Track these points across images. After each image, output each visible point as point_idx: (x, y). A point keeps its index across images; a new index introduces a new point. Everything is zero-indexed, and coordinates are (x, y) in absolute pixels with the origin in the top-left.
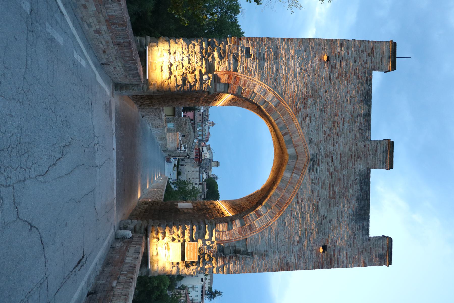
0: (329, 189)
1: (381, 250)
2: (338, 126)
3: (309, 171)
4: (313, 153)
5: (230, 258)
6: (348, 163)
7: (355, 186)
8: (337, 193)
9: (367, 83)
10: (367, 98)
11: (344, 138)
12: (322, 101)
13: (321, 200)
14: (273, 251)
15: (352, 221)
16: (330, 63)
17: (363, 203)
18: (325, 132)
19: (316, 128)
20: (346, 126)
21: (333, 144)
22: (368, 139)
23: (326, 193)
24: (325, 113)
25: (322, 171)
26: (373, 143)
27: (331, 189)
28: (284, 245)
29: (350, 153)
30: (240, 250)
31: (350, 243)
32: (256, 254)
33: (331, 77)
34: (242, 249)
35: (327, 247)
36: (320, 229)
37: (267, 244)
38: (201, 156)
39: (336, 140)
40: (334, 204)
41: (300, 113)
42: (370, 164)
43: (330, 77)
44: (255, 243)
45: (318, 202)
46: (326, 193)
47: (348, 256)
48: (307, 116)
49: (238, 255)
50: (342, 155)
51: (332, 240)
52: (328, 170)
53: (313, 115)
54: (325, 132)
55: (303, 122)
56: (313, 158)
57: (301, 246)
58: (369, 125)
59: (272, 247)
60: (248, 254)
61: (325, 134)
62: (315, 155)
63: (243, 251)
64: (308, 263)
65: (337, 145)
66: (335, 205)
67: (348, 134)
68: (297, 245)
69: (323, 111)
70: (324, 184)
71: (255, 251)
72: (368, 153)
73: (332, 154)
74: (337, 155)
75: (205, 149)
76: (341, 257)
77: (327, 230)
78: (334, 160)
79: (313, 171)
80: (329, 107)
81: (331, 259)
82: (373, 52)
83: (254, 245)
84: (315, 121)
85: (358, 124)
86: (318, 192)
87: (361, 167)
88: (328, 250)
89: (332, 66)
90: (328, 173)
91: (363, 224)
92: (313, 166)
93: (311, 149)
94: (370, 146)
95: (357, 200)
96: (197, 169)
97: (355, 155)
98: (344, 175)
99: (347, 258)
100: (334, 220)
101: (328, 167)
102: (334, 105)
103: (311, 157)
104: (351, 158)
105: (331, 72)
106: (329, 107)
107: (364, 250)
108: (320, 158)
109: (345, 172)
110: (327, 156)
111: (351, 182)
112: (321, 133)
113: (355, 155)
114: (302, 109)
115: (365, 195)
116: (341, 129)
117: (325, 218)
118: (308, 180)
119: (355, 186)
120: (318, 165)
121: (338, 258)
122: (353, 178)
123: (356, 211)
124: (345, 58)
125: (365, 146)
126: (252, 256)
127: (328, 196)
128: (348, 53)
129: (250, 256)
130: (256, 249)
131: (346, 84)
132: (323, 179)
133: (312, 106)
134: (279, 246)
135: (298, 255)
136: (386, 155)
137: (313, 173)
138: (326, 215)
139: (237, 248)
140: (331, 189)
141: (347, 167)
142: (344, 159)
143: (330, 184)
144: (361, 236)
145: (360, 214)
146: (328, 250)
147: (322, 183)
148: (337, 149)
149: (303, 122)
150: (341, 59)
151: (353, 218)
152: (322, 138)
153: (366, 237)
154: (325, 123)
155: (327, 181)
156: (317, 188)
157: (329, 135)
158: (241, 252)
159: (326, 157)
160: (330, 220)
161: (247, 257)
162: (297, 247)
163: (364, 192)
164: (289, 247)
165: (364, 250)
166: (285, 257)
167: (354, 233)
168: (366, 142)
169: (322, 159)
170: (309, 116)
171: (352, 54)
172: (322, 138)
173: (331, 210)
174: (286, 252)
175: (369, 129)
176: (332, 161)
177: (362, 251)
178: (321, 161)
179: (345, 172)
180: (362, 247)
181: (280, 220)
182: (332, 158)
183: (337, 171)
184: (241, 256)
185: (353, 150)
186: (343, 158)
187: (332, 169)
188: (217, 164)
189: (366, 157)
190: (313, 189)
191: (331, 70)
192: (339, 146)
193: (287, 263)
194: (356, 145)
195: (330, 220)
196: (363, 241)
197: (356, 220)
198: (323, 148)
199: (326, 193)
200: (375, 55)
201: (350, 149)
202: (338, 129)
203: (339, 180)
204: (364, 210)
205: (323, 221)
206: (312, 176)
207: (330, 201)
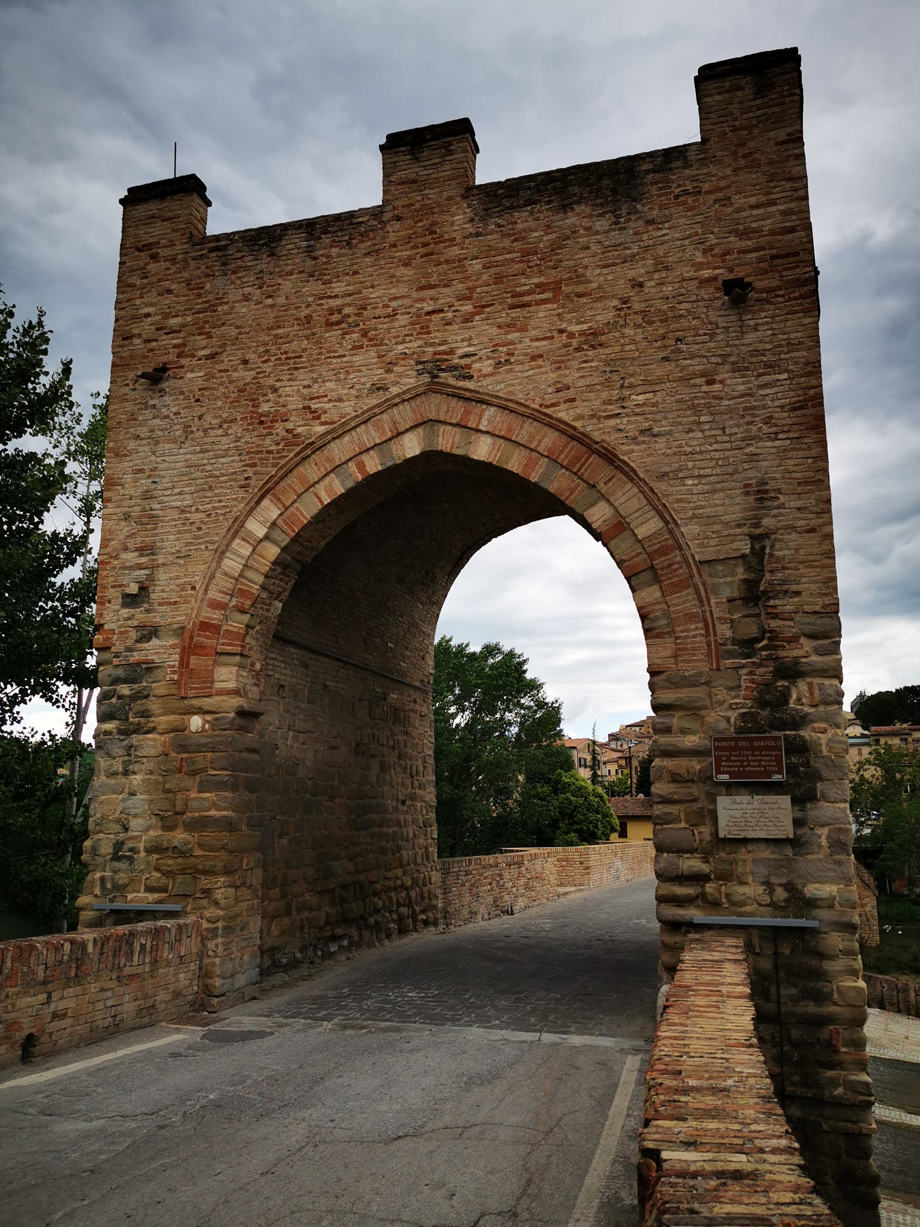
0: (528, 305)
1: (739, 94)
2: (340, 312)
3: (471, 377)
4: (415, 373)
5: (775, 616)
6: (447, 262)
7: (520, 226)
8: (542, 279)
9: (225, 248)
10: (265, 239)
11: (373, 287)
12: (269, 370)
13: (564, 326)
14: (746, 466)
15: (637, 212)
16: (170, 362)
17: (576, 190)
18: (354, 348)
19: (342, 376)
20: (339, 287)
21: (389, 316)
22: (376, 213)
23: (541, 314)
24: (301, 357)
25: (470, 339)
26: (389, 197)
27: (526, 299)
28: (724, 429)
29: (418, 261)
30: (745, 581)
31: (716, 201)
32: (757, 525)
33: (206, 352)
34: (741, 573)
35: (731, 276)
36: (665, 313)
37: (719, 486)
39: (378, 312)
40: (580, 283)
41: (299, 430)
42: (453, 193)
43: (207, 357)
44: (717, 527)
45: (571, 335)
46: (542, 312)
47: (763, 199)
48: (309, 408)
49: (762, 588)
51: (699, 267)
52: (466, 321)
53: (306, 391)
54: (354, 348)
55: (323, 419)
56: (429, 373)
57: (727, 367)
58: (338, 217)
59: (730, 469)
60: (758, 553)
61: (361, 347)
62: (420, 367)
63: (748, 569)
64: (793, 336)
65: (394, 304)
66: (579, 279)
67: (360, 277)
68: (722, 382)
69: (292, 362)
70: (510, 326)
71: (745, 530)
72: (417, 206)
73: (419, 316)
74: (422, 300)
76: (767, 225)
77: (668, 289)
78: (438, 307)
79: (469, 367)
80: (285, 347)
81: (773, 257)
82: (149, 246)
83: (726, 533)
84: (324, 382)
86: (538, 340)
87: (459, 220)
88: (741, 274)
89: (179, 356)
90: (477, 318)
91: (648, 172)
92: (455, 368)
93: (404, 381)
94: (397, 203)
95: (565, 208)
97: (425, 245)
98: (485, 267)
99: (773, 203)
100: (632, 274)
101: (459, 320)
102: (280, 331)
103: (426, 378)
104: (432, 254)
105: (193, 356)
106: (285, 347)
107: (741, 152)
108: (431, 349)
109: (477, 265)
110: (425, 330)
111: (507, 242)
112: (355, 358)
113: (425, 245)
114: (290, 426)
115: (549, 187)
116: (348, 300)
117: (625, 303)
118: (499, 378)
119: (520, 226)
120: (451, 352)
121: (772, 233)
122: (495, 236)
123: (602, 205)
124: (158, 322)
125: (399, 219)
126: (765, 536)
127: (549, 306)
128: (148, 315)
129: (768, 543)
130: (739, 526)
131: (225, 307)
132: (494, 331)
133: (280, 396)
134: (728, 445)
135: (760, 375)
136: (429, 151)
137: (476, 366)
138: (615, 303)
139: (736, 594)
140: (526, 299)
141: (460, 261)
142: (435, 274)
143: (512, 307)
144: (688, 172)
145: (614, 191)
146: (739, 273)
147: (508, 333)
148: (405, 301)
149: (323, 419)
150: (162, 332)
151: (624, 211)
152: (373, 353)
153: (692, 155)
154: (328, 352)
155: (503, 318)
156: (525, 344)
157: (365, 334)
158: (751, 576)
159: (429, 333)
160: (633, 287)
161: (771, 555)
162: (728, 382)
163: (539, 191)
164: (730, 410)
165: (741, 152)
166: (768, 420)
167: (677, 197)
168: (386, 217)
169: (432, 345)
170: (307, 403)
171: (152, 305)
172: (373, 353)
173: (600, 287)
174: (748, 418)
175: (351, 215)
176: (441, 311)
177: (745, 156)
178: (440, 345)
179: (477, 265)
180: (728, 160)
181: (632, 451)
182: (433, 312)
183: (471, 289)
184: (768, 576)
185: (408, 253)
186: (433, 280)
187: (464, 308)
189: (429, 210)
190: (528, 357)
191: (187, 356)
192: (395, 298)
193: (794, 409)
194: (395, 246)
195: (633, 287)
196: (703, 162)
197: (634, 200)
198: (400, 347)
199: (541, 314)
200: (155, 240)
201: (407, 264)
202: (346, 311)
203: (498, 279)
204: (599, 179)
205: (637, 307)
206: (486, 366)
207: (568, 297)
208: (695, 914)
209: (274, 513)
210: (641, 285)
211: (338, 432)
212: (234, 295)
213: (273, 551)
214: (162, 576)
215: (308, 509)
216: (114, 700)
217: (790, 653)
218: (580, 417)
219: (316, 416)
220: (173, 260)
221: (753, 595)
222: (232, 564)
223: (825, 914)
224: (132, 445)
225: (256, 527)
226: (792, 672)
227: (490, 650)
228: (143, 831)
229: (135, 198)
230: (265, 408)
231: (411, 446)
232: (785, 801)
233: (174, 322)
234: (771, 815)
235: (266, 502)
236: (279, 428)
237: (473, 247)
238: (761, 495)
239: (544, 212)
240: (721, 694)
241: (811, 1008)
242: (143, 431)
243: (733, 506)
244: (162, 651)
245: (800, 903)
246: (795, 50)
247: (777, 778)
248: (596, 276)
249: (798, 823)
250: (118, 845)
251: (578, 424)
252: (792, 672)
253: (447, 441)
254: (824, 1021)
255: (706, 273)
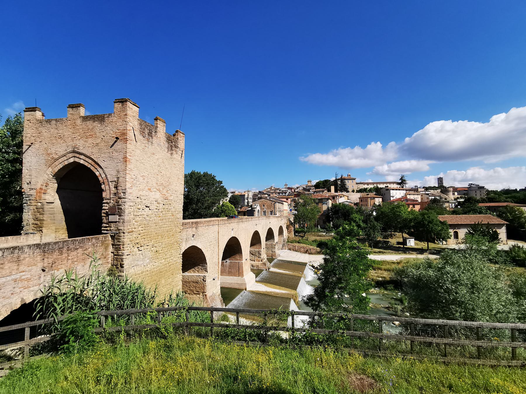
60: (118, 180)
70: (85, 141)
75: (296, 191)
109: (81, 130)
179: (81, 130)
206: (82, 148)
211: (60, 158)
212: (43, 131)
214: (33, 180)
215: (56, 170)
220: (33, 123)
223: (121, 231)
224: (27, 157)
227: (206, 175)
228: (31, 221)
231: (72, 160)
236: (51, 156)
237: (81, 127)
238: (118, 172)
239: (91, 122)
240: (112, 201)
241: (118, 243)
242: (29, 154)
243: (114, 173)
248: (98, 134)
252: (120, 198)
253: (77, 160)
254: (120, 245)
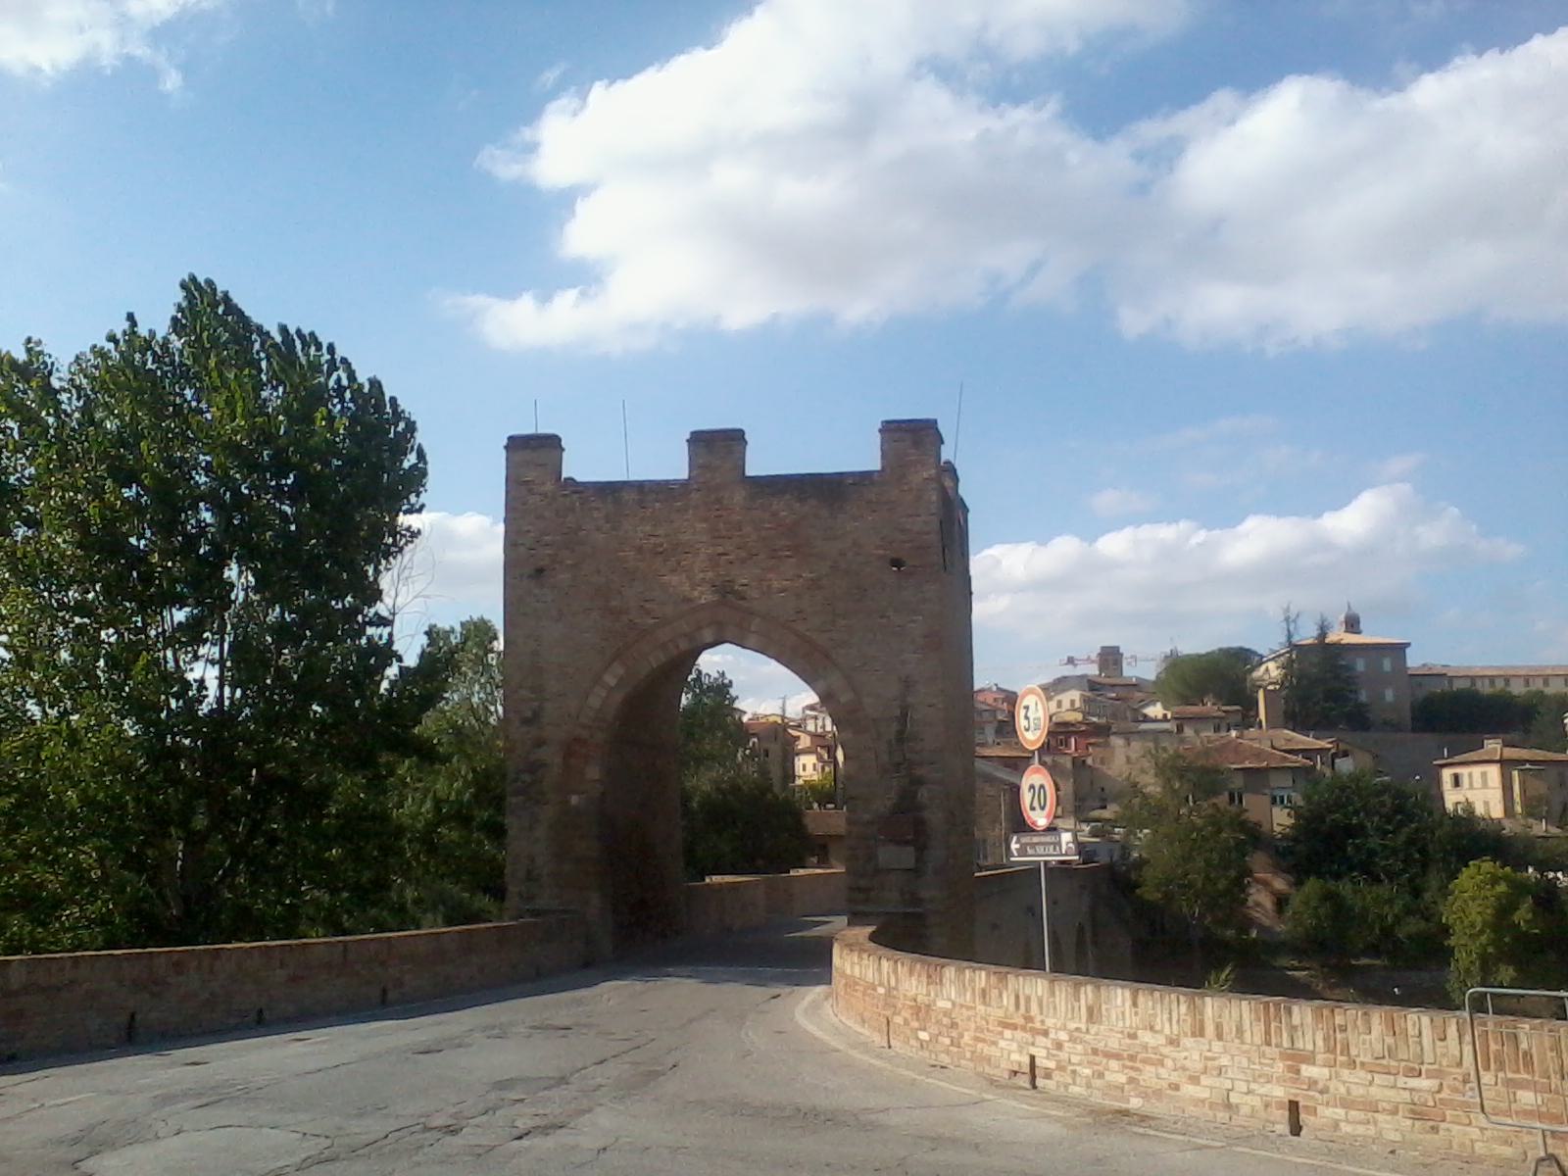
27: (780, 553)
34: (895, 727)
38: (1066, 724)
50: (716, 534)
51: (878, 547)
60: (904, 715)
85: (657, 505)
87: (739, 496)
96: (1117, 742)
128: (528, 531)
136: (718, 448)
140: (780, 553)
188: (1110, 657)
208: (861, 908)
209: (621, 671)
210: (845, 555)
213: (619, 697)
216: (519, 783)
217: (919, 772)
218: (808, 630)
219: (648, 613)
221: (901, 737)
222: (594, 702)
225: (610, 680)
226: (919, 782)
229: (515, 444)
230: (614, 603)
232: (911, 849)
233: (547, 538)
234: (906, 856)
235: (615, 664)
238: (908, 684)
244: (551, 755)
245: (916, 900)
246: (935, 421)
247: (909, 837)
249: (918, 860)
250: (529, 872)
251: (808, 633)
252: (919, 782)
255: (881, 552)
